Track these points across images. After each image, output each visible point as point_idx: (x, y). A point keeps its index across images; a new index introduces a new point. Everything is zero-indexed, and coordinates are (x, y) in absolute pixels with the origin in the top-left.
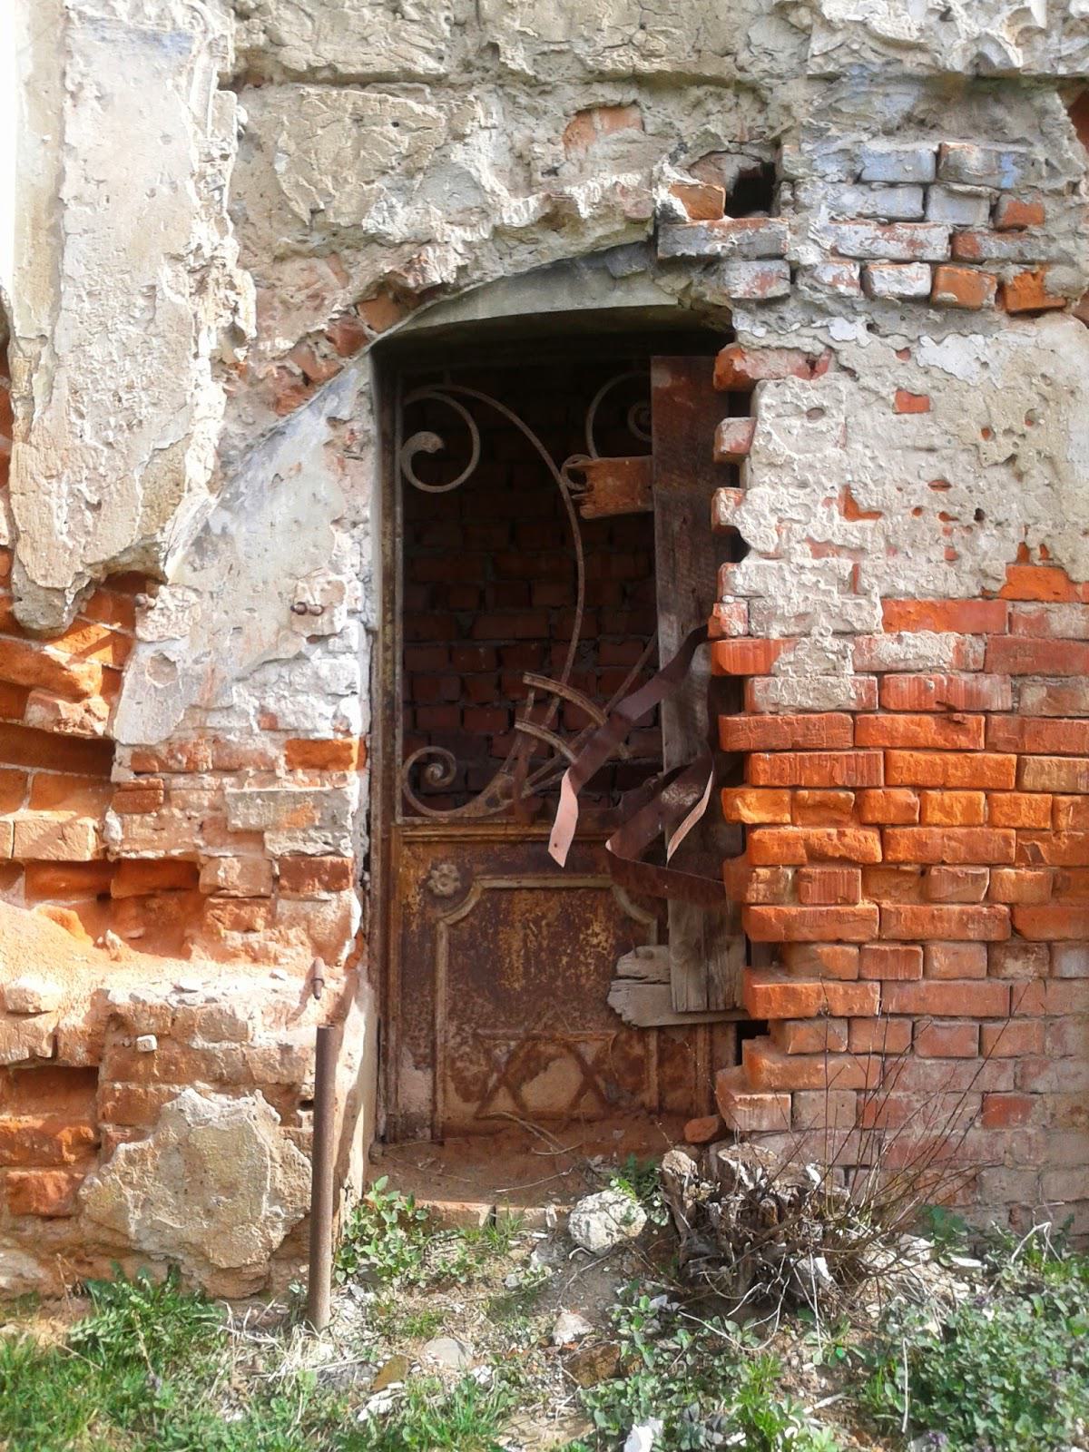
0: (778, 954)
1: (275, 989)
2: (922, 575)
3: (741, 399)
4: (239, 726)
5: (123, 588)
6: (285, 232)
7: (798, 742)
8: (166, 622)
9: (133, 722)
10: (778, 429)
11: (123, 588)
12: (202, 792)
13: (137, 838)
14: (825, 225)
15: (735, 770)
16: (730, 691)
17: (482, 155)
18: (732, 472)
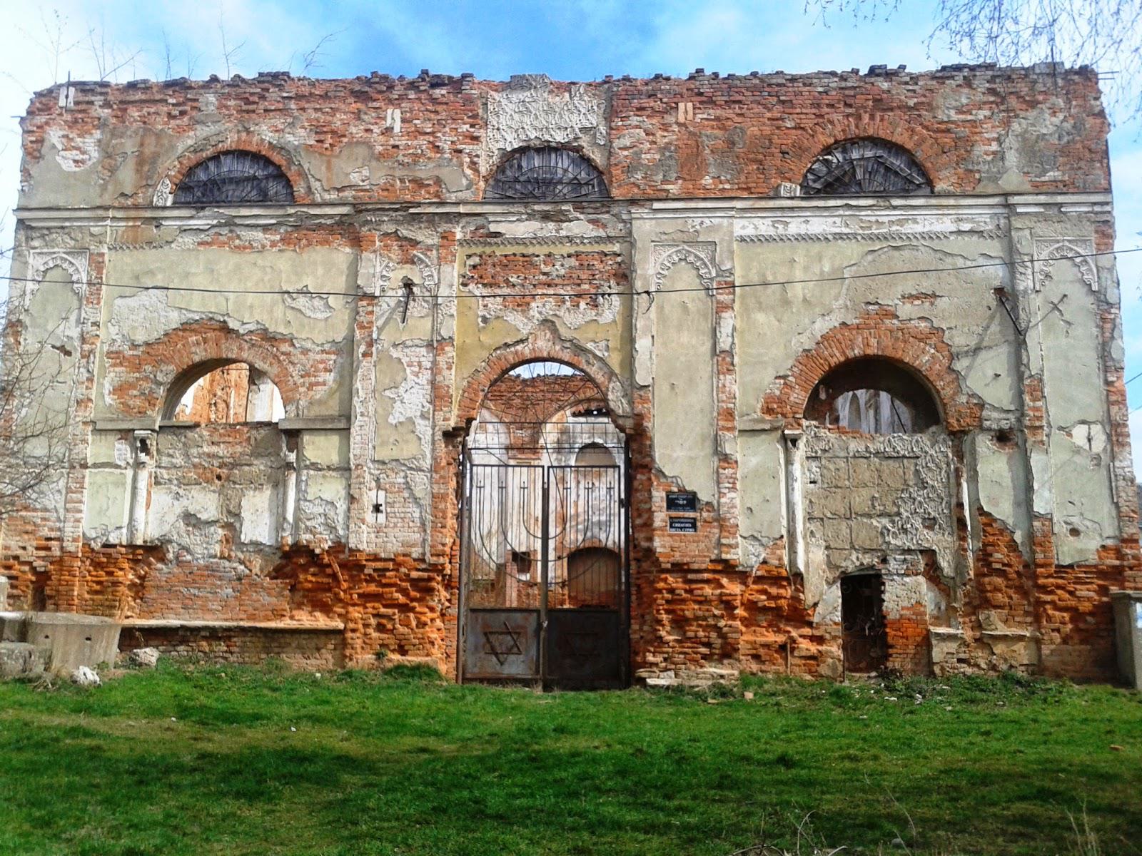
0: (892, 647)
1: (835, 649)
2: (906, 604)
3: (884, 584)
4: (827, 620)
5: (816, 605)
6: (831, 565)
7: (894, 622)
8: (819, 609)
9: (816, 619)
10: (888, 587)
11: (816, 605)
12: (823, 628)
13: (816, 633)
14: (893, 565)
15: (885, 626)
16: (884, 617)
17: (854, 557)
18: (883, 592)
